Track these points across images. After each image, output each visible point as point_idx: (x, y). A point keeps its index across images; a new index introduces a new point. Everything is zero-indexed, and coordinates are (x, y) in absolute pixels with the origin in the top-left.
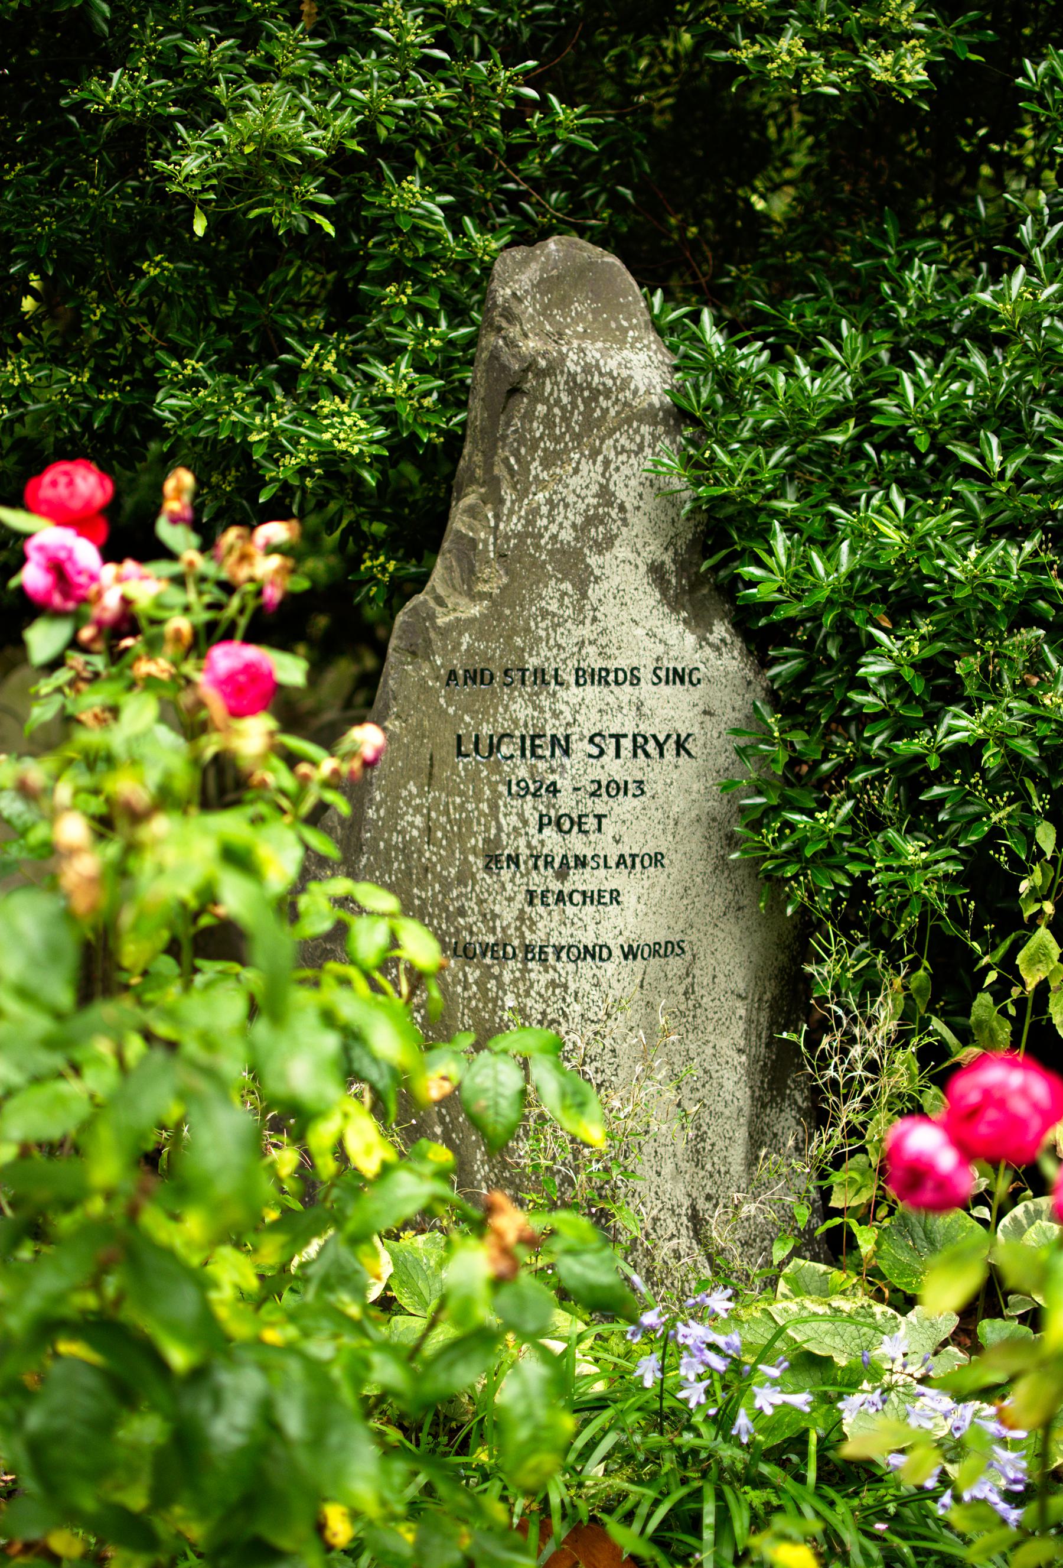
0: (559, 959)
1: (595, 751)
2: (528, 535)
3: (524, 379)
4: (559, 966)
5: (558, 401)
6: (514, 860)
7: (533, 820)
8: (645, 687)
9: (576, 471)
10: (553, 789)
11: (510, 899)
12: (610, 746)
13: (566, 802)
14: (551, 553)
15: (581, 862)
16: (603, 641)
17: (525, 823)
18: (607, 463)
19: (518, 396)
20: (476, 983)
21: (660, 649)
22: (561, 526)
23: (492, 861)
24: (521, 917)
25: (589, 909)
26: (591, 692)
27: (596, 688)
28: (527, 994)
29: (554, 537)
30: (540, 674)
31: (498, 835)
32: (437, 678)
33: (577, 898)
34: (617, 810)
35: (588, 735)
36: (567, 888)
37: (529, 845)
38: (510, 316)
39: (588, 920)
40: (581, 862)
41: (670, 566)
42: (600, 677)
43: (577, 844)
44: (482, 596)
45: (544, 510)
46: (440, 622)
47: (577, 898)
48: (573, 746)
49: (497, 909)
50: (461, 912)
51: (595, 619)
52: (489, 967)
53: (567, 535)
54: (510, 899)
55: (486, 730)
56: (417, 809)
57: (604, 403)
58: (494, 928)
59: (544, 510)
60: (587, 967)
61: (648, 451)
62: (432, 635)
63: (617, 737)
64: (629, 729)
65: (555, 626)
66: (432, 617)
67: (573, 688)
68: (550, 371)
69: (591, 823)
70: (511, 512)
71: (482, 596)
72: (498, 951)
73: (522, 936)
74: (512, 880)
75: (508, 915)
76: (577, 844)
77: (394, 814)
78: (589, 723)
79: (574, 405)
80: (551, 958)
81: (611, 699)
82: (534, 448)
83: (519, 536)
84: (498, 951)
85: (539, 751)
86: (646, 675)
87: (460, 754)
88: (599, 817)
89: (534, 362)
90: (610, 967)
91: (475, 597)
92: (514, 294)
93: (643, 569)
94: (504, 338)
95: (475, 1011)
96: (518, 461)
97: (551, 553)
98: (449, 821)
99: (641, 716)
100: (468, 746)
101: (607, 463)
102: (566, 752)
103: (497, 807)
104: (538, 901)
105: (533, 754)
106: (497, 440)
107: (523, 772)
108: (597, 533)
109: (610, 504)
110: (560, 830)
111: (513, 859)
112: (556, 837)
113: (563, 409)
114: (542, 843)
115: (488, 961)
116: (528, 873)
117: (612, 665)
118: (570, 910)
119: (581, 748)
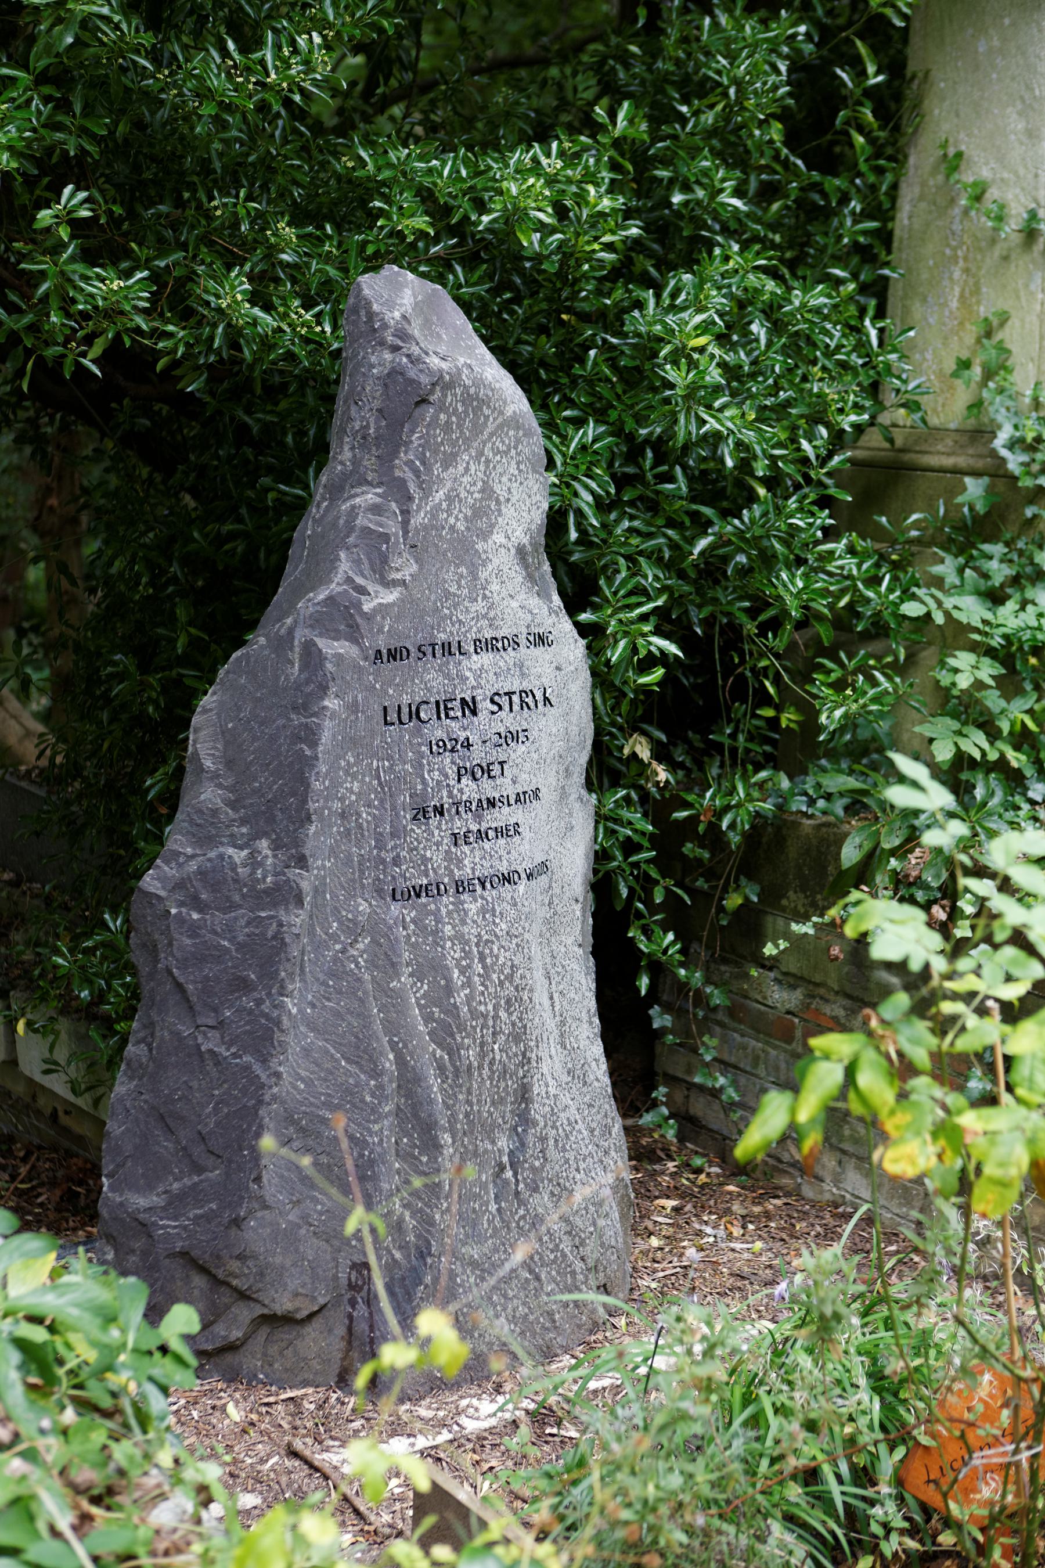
0: (484, 888)
1: (495, 708)
2: (433, 527)
3: (432, 392)
4: (486, 894)
5: (456, 410)
6: (440, 811)
7: (452, 772)
8: (522, 649)
9: (467, 469)
10: (468, 745)
11: (438, 844)
12: (504, 701)
13: (478, 755)
14: (450, 542)
15: (492, 803)
16: (492, 614)
17: (446, 776)
18: (488, 461)
19: (424, 406)
20: (413, 921)
21: (529, 617)
22: (457, 519)
23: (421, 813)
24: (448, 856)
25: (502, 841)
26: (486, 659)
27: (491, 655)
28: (463, 922)
29: (452, 528)
30: (447, 648)
31: (425, 789)
32: (366, 659)
33: (491, 834)
34: (513, 756)
35: (489, 694)
36: (484, 826)
37: (450, 795)
38: (403, 335)
39: (502, 852)
40: (492, 803)
41: (529, 548)
42: (490, 645)
43: (488, 789)
44: (395, 583)
45: (444, 505)
46: (366, 607)
47: (491, 834)
48: (479, 706)
49: (428, 854)
50: (397, 861)
51: (485, 597)
52: (425, 905)
53: (461, 526)
54: (438, 844)
55: (406, 699)
56: (354, 776)
57: (486, 412)
58: (426, 870)
59: (444, 505)
60: (506, 890)
61: (513, 452)
62: (359, 620)
63: (509, 694)
64: (516, 687)
65: (456, 606)
66: (358, 605)
67: (475, 657)
68: (449, 386)
69: (496, 769)
70: (419, 508)
71: (395, 583)
72: (432, 890)
73: (451, 873)
74: (439, 828)
75: (437, 857)
76: (488, 789)
77: (336, 784)
78: (492, 684)
79: (466, 412)
80: (478, 888)
81: (502, 664)
82: (436, 452)
83: (425, 528)
84: (432, 890)
85: (452, 713)
86: (523, 641)
87: (386, 723)
88: (501, 763)
89: (441, 377)
90: (521, 888)
91: (389, 584)
92: (404, 317)
93: (513, 551)
94: (408, 356)
95: (415, 946)
96: (423, 463)
97: (450, 542)
98: (380, 784)
99: (523, 675)
100: (393, 717)
101: (488, 461)
102: (474, 713)
103: (421, 765)
104: (461, 842)
105: (447, 716)
106: (398, 446)
107: (439, 734)
108: (482, 524)
109: (490, 498)
110: (475, 779)
111: (440, 811)
112: (473, 785)
113: (459, 417)
114: (461, 791)
115: (423, 900)
116: (452, 820)
117: (499, 634)
118: (487, 845)
119: (485, 706)
